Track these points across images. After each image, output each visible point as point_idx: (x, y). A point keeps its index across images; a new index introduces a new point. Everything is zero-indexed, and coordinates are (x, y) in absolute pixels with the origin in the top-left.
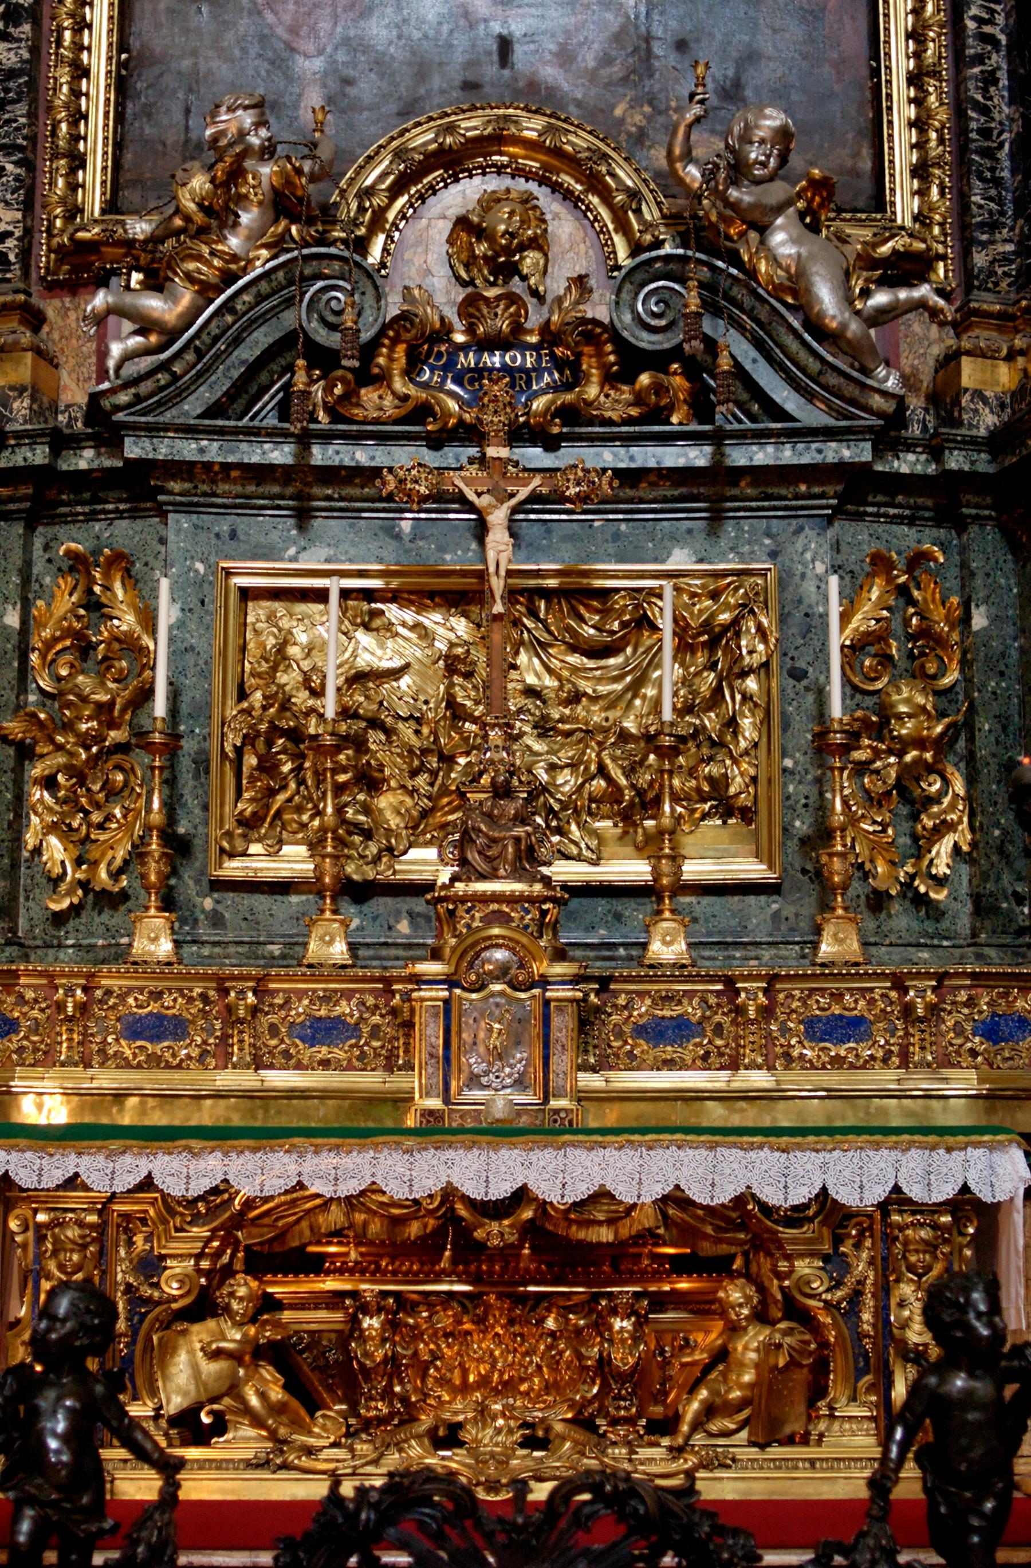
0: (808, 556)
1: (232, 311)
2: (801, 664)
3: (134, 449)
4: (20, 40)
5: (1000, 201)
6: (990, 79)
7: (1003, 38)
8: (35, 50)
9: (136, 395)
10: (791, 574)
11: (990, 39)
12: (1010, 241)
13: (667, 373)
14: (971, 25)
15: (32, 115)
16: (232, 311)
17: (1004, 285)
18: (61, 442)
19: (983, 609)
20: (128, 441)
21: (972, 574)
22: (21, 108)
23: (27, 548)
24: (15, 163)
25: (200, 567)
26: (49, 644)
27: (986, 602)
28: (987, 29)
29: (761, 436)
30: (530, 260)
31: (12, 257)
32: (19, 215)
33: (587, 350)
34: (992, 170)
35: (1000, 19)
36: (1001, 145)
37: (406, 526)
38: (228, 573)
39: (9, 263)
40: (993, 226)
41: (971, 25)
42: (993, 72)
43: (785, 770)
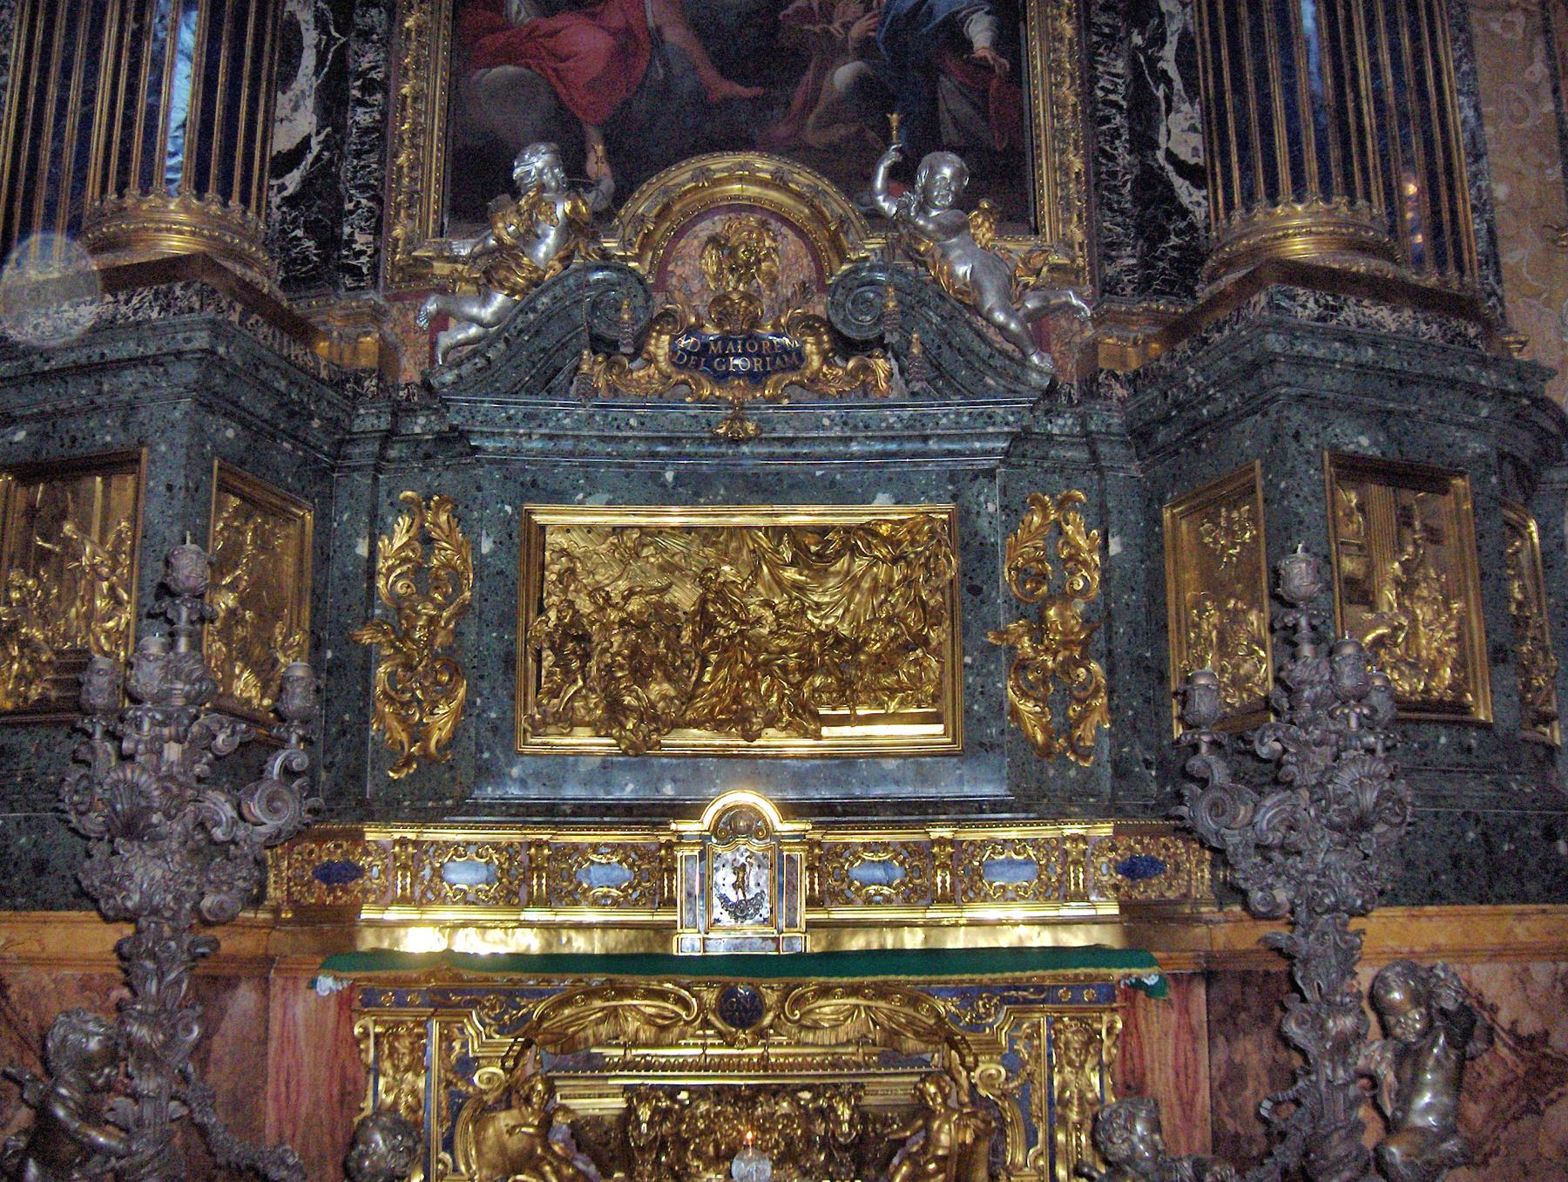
0: (982, 499)
1: (534, 310)
2: (977, 582)
4: (372, 106)
5: (1124, 225)
6: (1116, 134)
7: (1125, 104)
8: (384, 114)
9: (460, 376)
10: (968, 512)
11: (1115, 104)
12: (1133, 256)
13: (870, 357)
15: (381, 162)
16: (534, 310)
17: (1129, 290)
18: (401, 411)
19: (1117, 539)
21: (1109, 512)
22: (374, 157)
23: (375, 494)
24: (369, 199)
25: (508, 508)
26: (391, 569)
27: (1119, 533)
28: (1112, 97)
31: (365, 270)
33: (810, 339)
34: (1119, 202)
35: (1121, 89)
36: (1124, 185)
37: (669, 476)
38: (530, 512)
39: (362, 274)
41: (1100, 94)
42: (1117, 129)
43: (965, 665)
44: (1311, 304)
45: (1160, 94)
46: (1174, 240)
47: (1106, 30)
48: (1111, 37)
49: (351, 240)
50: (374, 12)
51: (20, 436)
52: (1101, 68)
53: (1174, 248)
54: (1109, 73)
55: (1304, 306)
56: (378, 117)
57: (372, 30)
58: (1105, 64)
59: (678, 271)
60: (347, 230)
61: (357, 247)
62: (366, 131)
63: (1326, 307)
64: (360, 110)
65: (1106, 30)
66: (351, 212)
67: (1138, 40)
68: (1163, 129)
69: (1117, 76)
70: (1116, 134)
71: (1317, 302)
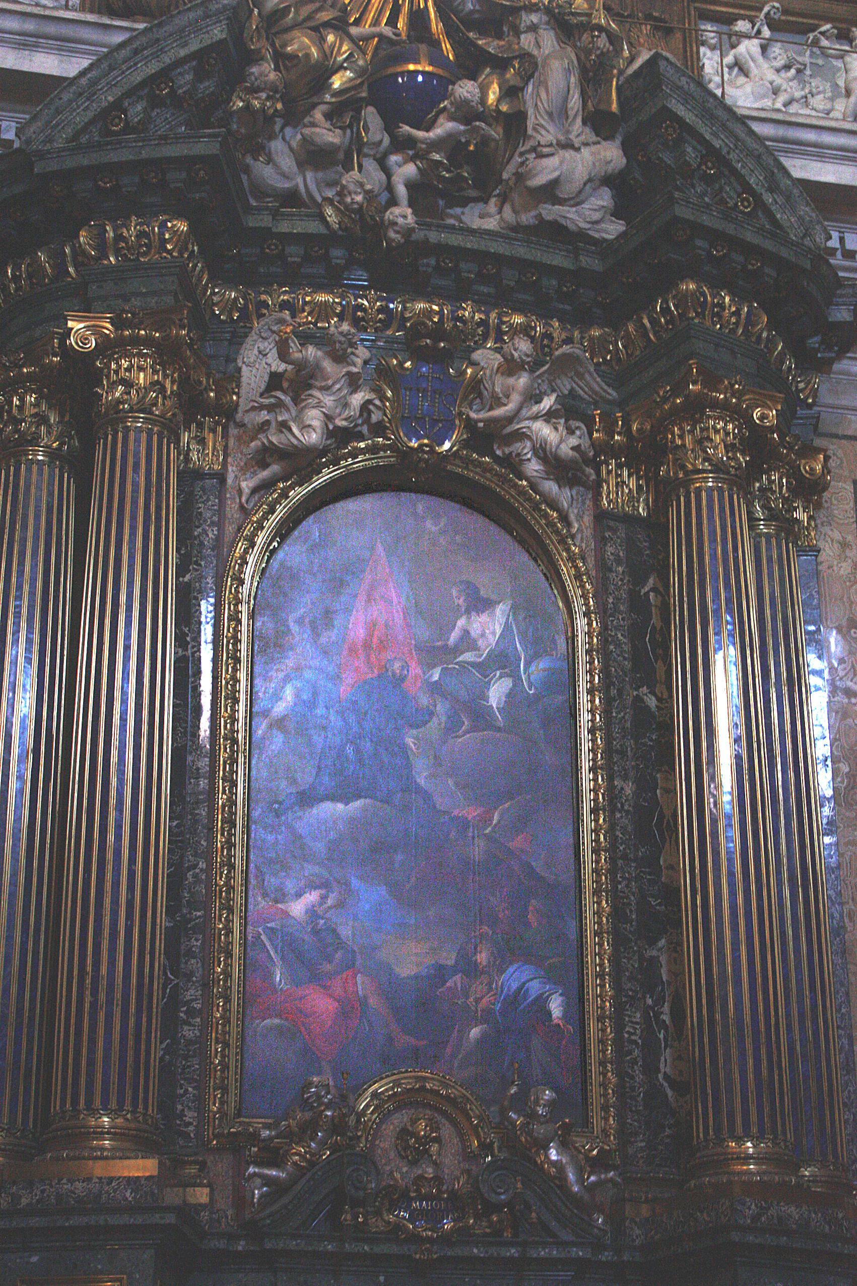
3: (268, 1245)
6: (634, 1062)
7: (640, 1041)
11: (635, 1042)
14: (626, 1035)
20: (266, 1240)
22: (196, 1061)
24: (193, 1088)
28: (633, 1037)
29: (545, 1245)
30: (435, 1148)
31: (192, 1135)
32: (196, 1115)
34: (636, 1106)
40: (636, 1134)
41: (626, 1035)
44: (753, 1206)
45: (662, 1036)
46: (668, 1131)
47: (630, 993)
48: (632, 998)
49: (182, 1115)
50: (193, 961)
51: (34, 1259)
52: (627, 1019)
53: (668, 1136)
54: (632, 1022)
55: (749, 1208)
56: (198, 1034)
57: (192, 974)
58: (630, 1016)
59: (382, 1145)
60: (179, 1107)
61: (187, 1119)
62: (190, 1042)
63: (761, 1207)
64: (186, 1028)
65: (630, 993)
66: (182, 1096)
67: (649, 1001)
68: (663, 1059)
69: (637, 1023)
70: (634, 1062)
71: (756, 1205)
